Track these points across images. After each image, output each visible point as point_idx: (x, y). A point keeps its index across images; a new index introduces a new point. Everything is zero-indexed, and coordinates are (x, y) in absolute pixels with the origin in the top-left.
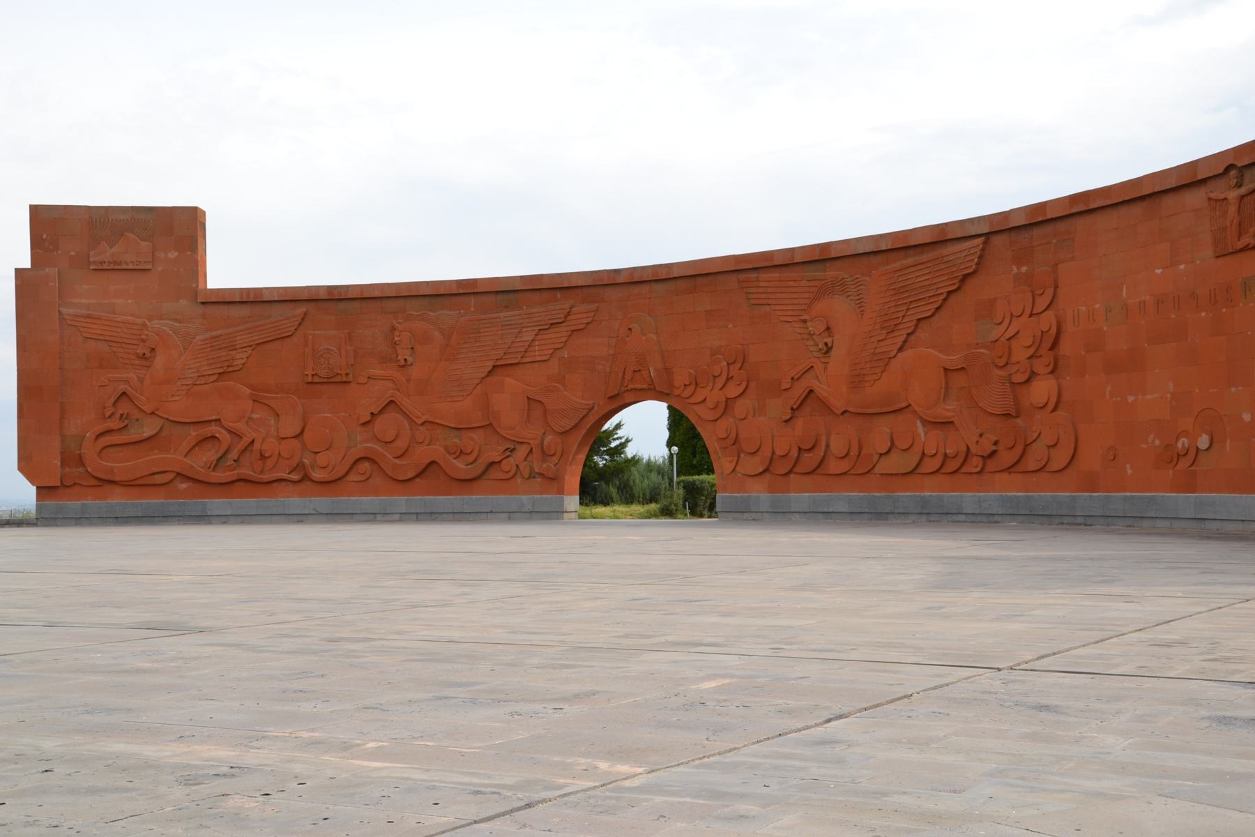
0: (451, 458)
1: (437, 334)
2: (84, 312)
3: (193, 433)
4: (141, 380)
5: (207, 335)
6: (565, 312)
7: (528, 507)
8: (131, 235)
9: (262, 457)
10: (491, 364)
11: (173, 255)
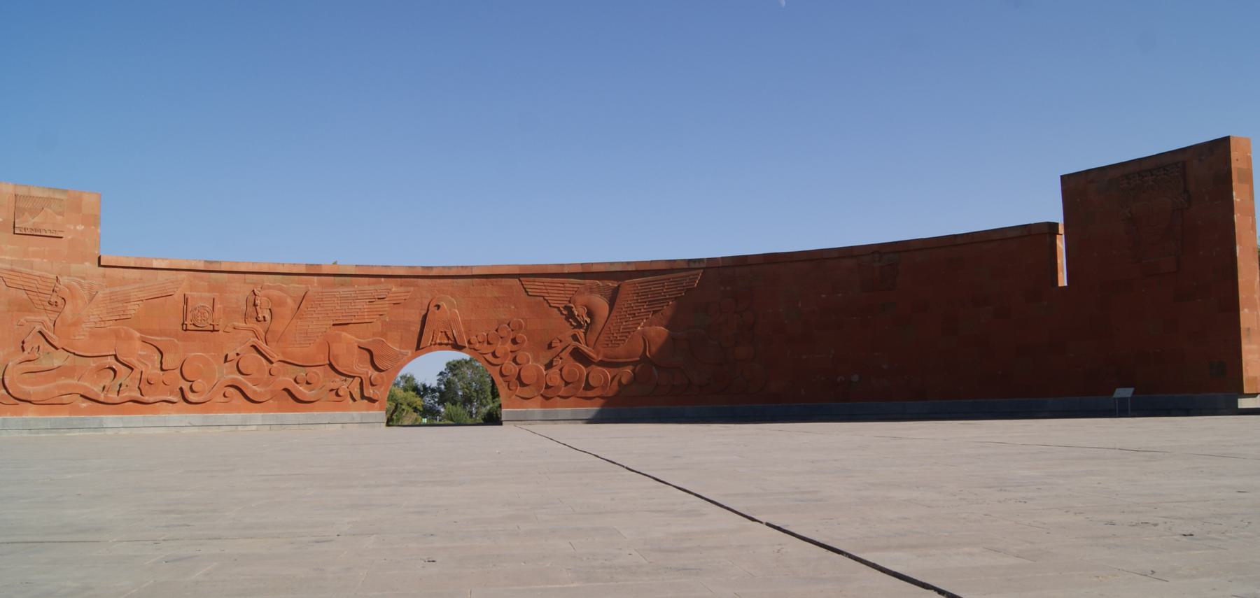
1: (289, 300)
2: (8, 267)
5: (107, 291)
7: (358, 420)
8: (49, 211)
11: (80, 227)
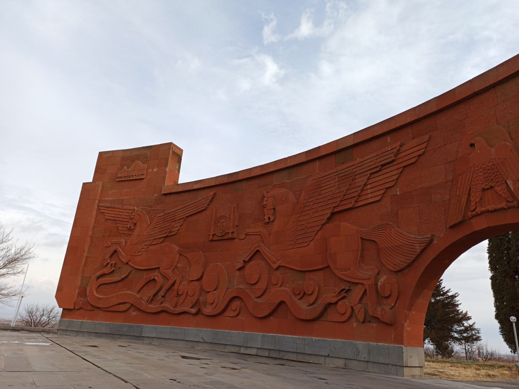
0: (296, 299)
3: (146, 276)
4: (126, 242)
6: (395, 150)
7: (363, 356)
9: (178, 295)
10: (329, 212)
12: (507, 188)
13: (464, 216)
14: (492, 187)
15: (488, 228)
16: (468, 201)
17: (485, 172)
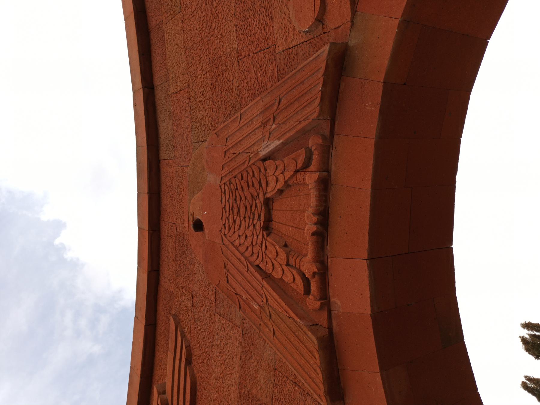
12: (274, 159)
13: (314, 326)
14: (268, 202)
15: (375, 259)
16: (279, 286)
17: (236, 210)
